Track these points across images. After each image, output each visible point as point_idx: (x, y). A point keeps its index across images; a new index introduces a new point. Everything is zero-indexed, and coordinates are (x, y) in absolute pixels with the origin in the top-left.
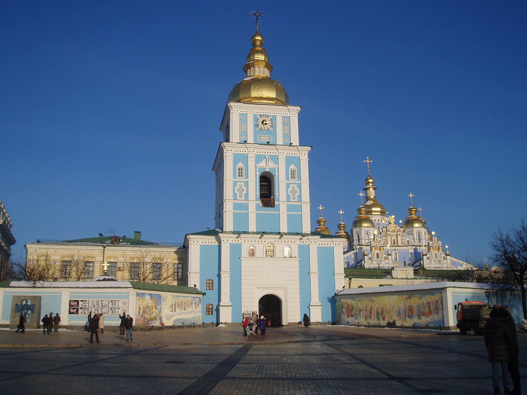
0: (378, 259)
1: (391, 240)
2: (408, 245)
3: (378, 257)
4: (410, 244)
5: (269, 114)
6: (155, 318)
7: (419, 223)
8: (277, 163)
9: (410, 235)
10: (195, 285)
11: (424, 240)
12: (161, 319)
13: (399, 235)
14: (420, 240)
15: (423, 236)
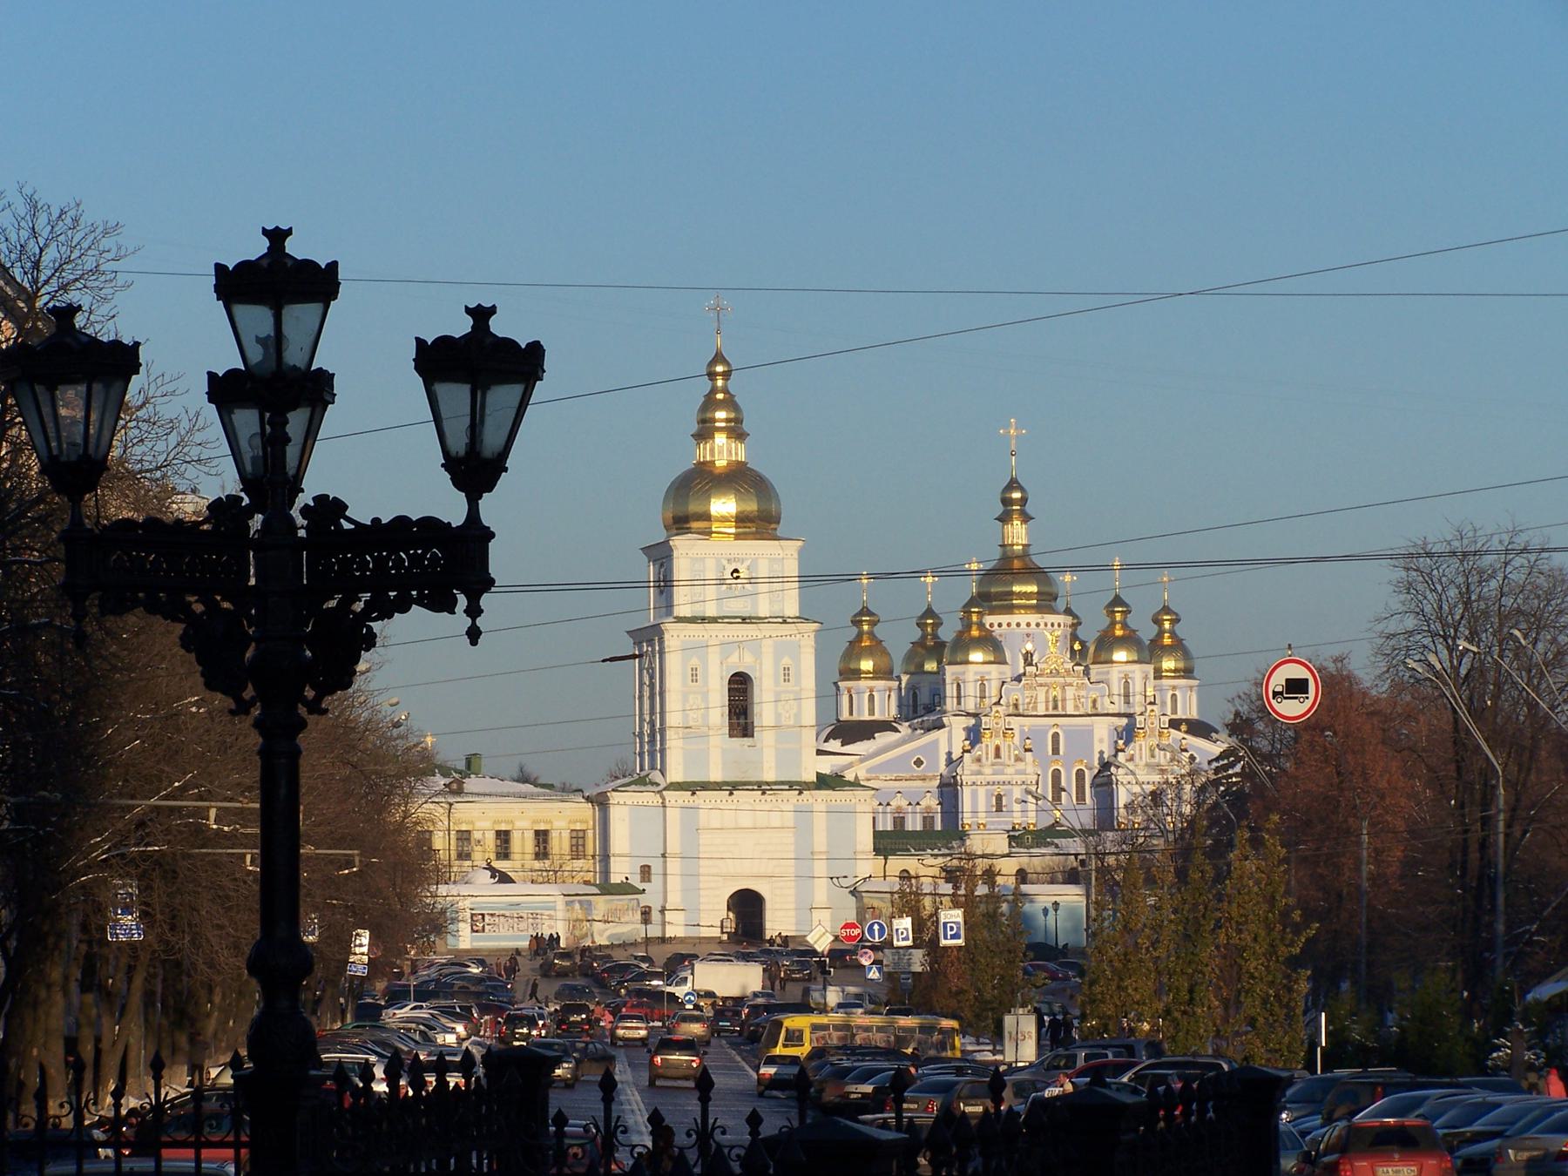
0: (999, 760)
1: (1047, 698)
2: (1094, 712)
3: (998, 755)
4: (1100, 711)
5: (744, 556)
6: (586, 935)
7: (1128, 649)
8: (758, 654)
9: (1102, 685)
10: (627, 878)
11: (1139, 698)
12: (592, 935)
13: (1071, 685)
14: (1127, 696)
15: (1137, 686)
